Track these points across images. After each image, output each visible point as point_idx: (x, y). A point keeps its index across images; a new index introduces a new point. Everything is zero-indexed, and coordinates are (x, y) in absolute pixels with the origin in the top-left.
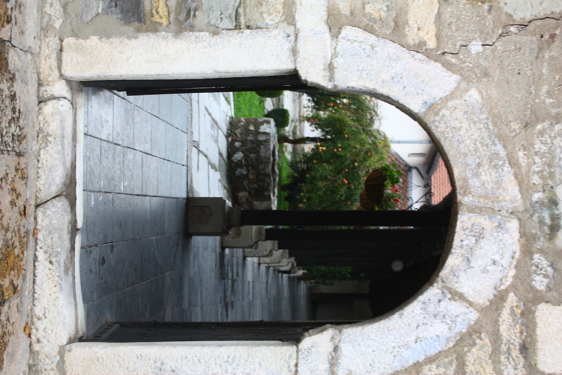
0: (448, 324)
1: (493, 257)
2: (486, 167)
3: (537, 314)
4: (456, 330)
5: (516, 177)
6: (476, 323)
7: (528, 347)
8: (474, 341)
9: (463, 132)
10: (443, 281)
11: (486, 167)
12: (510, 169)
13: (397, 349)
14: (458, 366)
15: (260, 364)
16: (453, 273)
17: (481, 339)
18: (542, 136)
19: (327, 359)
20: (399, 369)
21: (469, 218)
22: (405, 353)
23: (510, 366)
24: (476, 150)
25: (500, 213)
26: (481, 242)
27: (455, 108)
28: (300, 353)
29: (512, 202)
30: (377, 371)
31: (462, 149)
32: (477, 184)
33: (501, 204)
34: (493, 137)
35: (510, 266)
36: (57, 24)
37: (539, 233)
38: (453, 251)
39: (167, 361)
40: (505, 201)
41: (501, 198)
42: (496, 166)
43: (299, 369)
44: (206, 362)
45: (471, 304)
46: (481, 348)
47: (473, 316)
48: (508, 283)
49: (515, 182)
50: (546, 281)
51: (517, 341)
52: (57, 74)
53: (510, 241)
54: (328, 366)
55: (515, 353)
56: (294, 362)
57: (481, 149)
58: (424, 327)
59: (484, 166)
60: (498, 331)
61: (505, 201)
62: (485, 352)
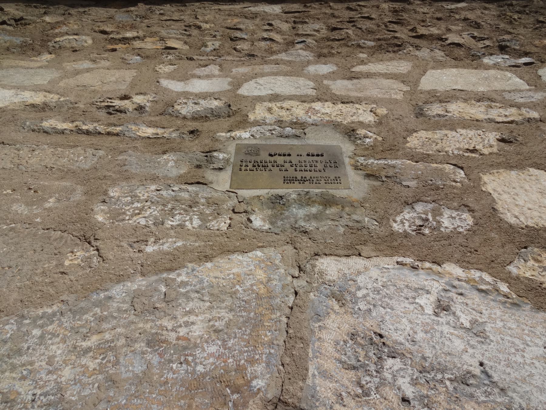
1: (429, 310)
2: (167, 323)
5: (208, 258)
11: (167, 323)
12: (183, 271)
18: (124, 213)
21: (325, 374)
24: (105, 348)
25: (301, 292)
26: (396, 342)
29: (269, 265)
31: (87, 392)
32: (213, 349)
33: (278, 289)
34: (83, 304)
40: (269, 280)
41: (263, 291)
48: (488, 278)
49: (221, 261)
53: (374, 273)
57: (107, 336)
59: (162, 327)
61: (269, 280)
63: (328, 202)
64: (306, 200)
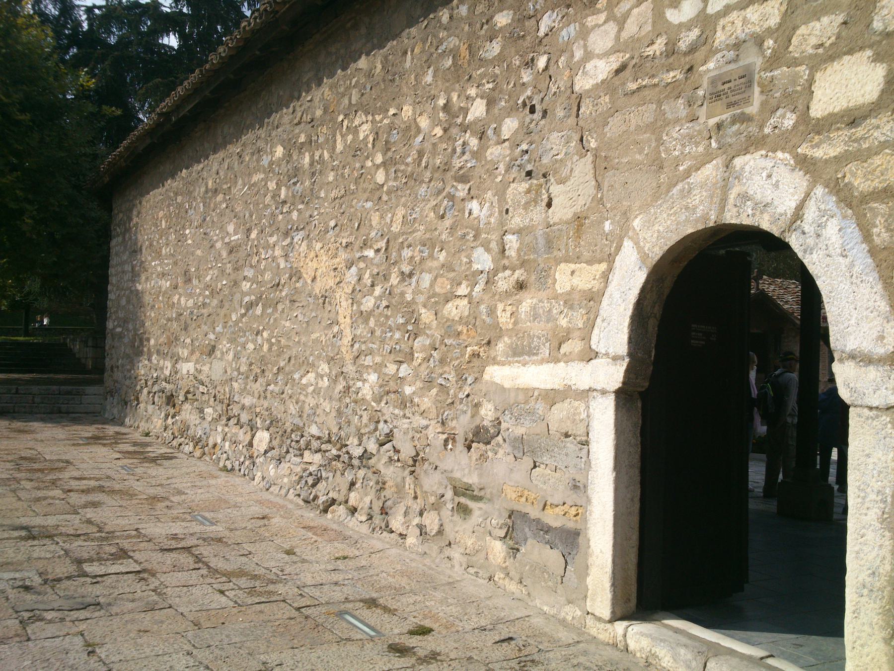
0: (828, 219)
2: (689, 201)
3: (819, 116)
4: (834, 208)
5: (699, 169)
6: (827, 186)
7: (853, 118)
8: (846, 185)
9: (661, 229)
10: (784, 231)
11: (689, 201)
13: (854, 280)
14: (875, 200)
15: (868, 456)
16: (775, 221)
17: (844, 177)
19: (864, 369)
20: (877, 276)
21: (729, 211)
22: (857, 269)
23: (875, 134)
24: (675, 213)
27: (645, 239)
28: (856, 403)
30: (878, 303)
32: (701, 208)
35: (774, 158)
36: (579, 613)
37: (745, 134)
38: (756, 224)
39: (860, 579)
42: (689, 192)
43: (874, 405)
44: (864, 527)
45: (807, 195)
46: (854, 175)
47: (819, 191)
50: (789, 115)
51: (846, 133)
52: (608, 626)
54: (871, 368)
55: (860, 131)
56: (866, 411)
58: (831, 248)
60: (835, 157)
62: (857, 170)
63: (744, 119)
64: (733, 122)
